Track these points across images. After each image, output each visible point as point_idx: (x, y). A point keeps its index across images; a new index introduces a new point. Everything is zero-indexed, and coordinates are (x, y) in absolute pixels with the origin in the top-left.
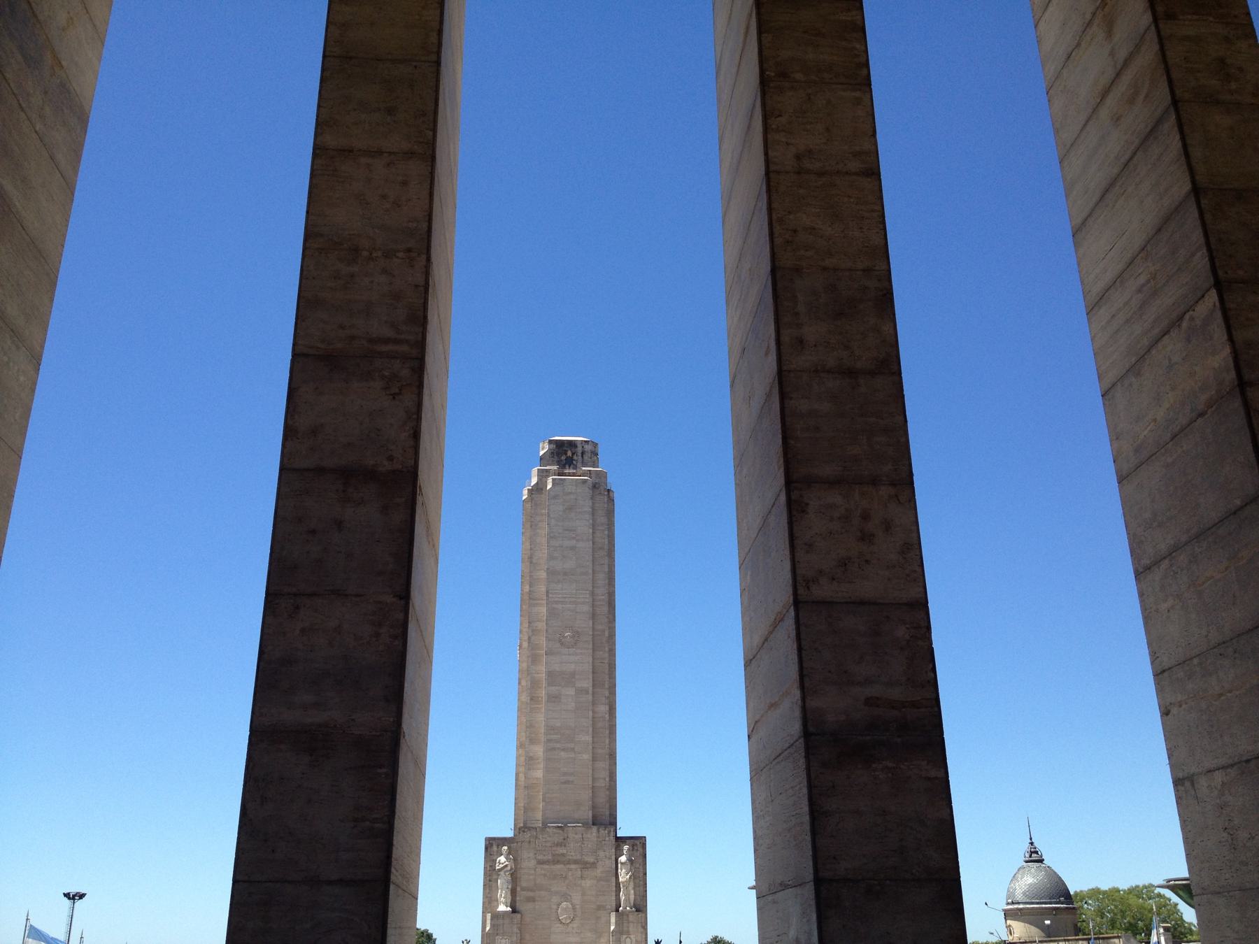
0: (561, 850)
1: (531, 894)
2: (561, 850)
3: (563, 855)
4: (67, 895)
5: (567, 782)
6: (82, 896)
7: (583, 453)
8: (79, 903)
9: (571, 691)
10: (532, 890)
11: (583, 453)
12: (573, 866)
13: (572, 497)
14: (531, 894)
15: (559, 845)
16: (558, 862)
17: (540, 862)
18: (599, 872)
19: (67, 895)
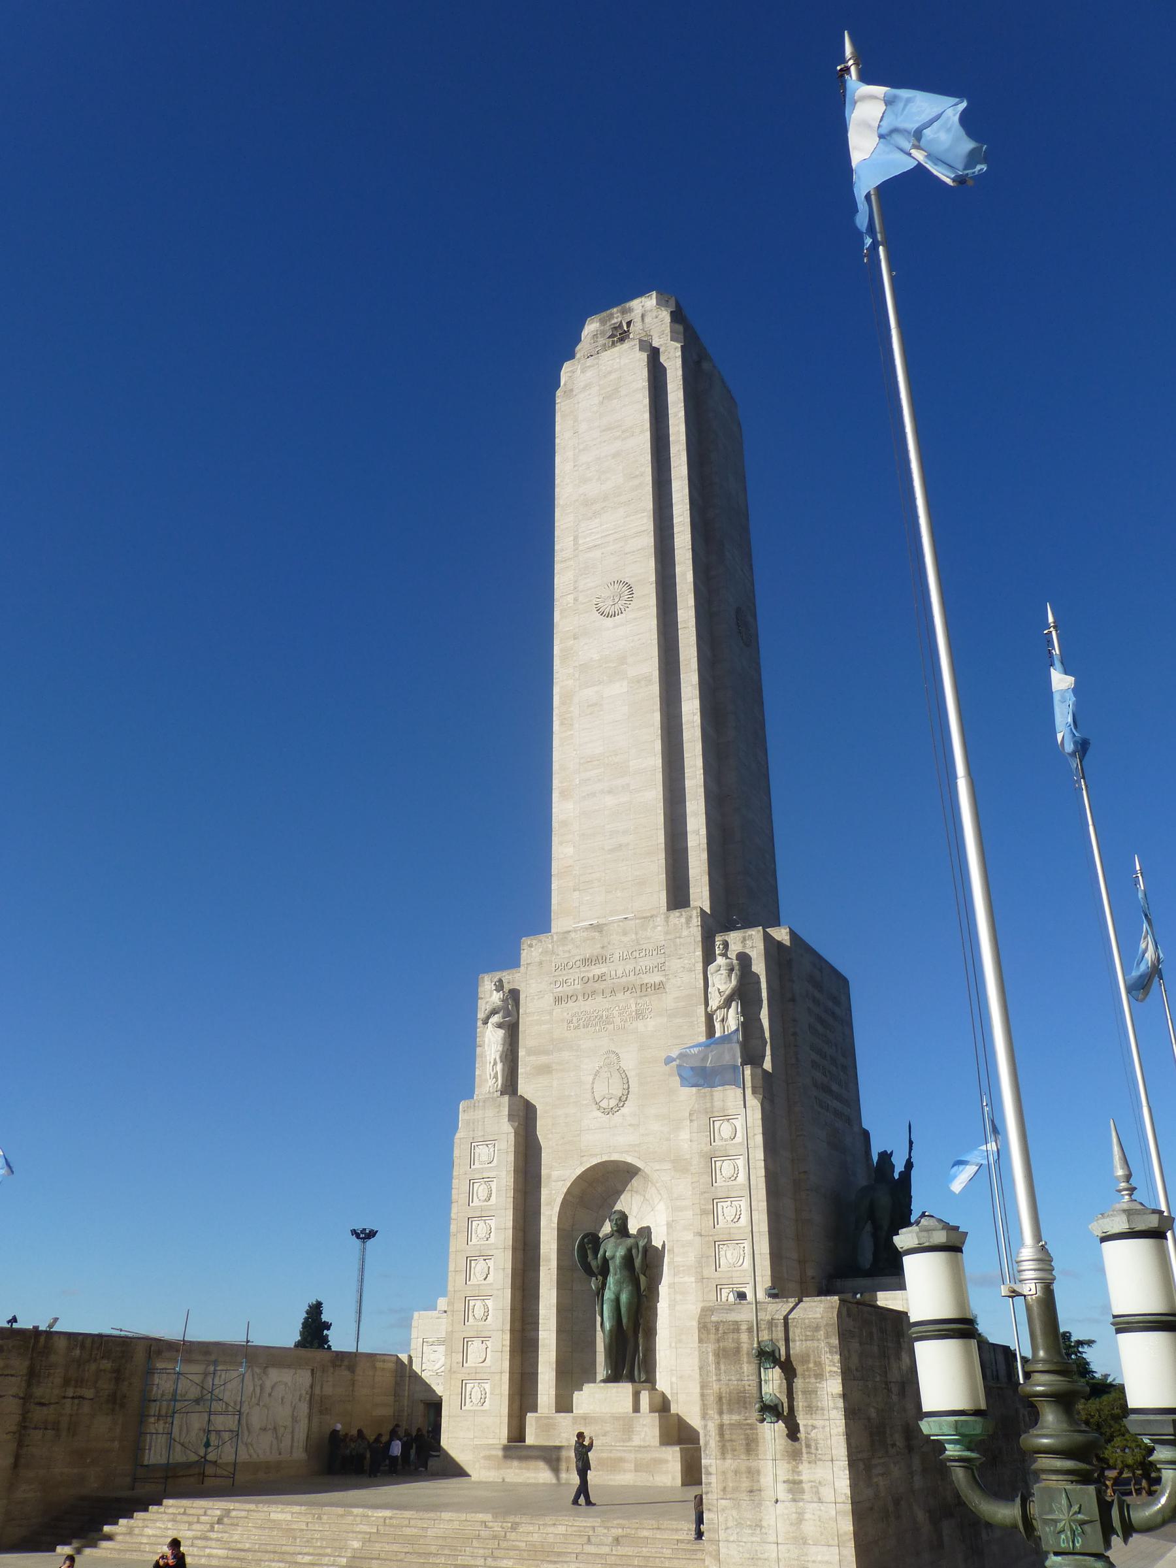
0: (597, 970)
1: (544, 1059)
2: (597, 970)
3: (601, 978)
4: (354, 1232)
5: (620, 847)
6: (372, 1234)
7: (643, 316)
8: (370, 1243)
9: (619, 688)
10: (547, 1052)
11: (643, 316)
12: (620, 996)
13: (613, 376)
14: (544, 1059)
15: (587, 961)
16: (594, 992)
17: (558, 1000)
18: (669, 1000)
19: (354, 1232)
